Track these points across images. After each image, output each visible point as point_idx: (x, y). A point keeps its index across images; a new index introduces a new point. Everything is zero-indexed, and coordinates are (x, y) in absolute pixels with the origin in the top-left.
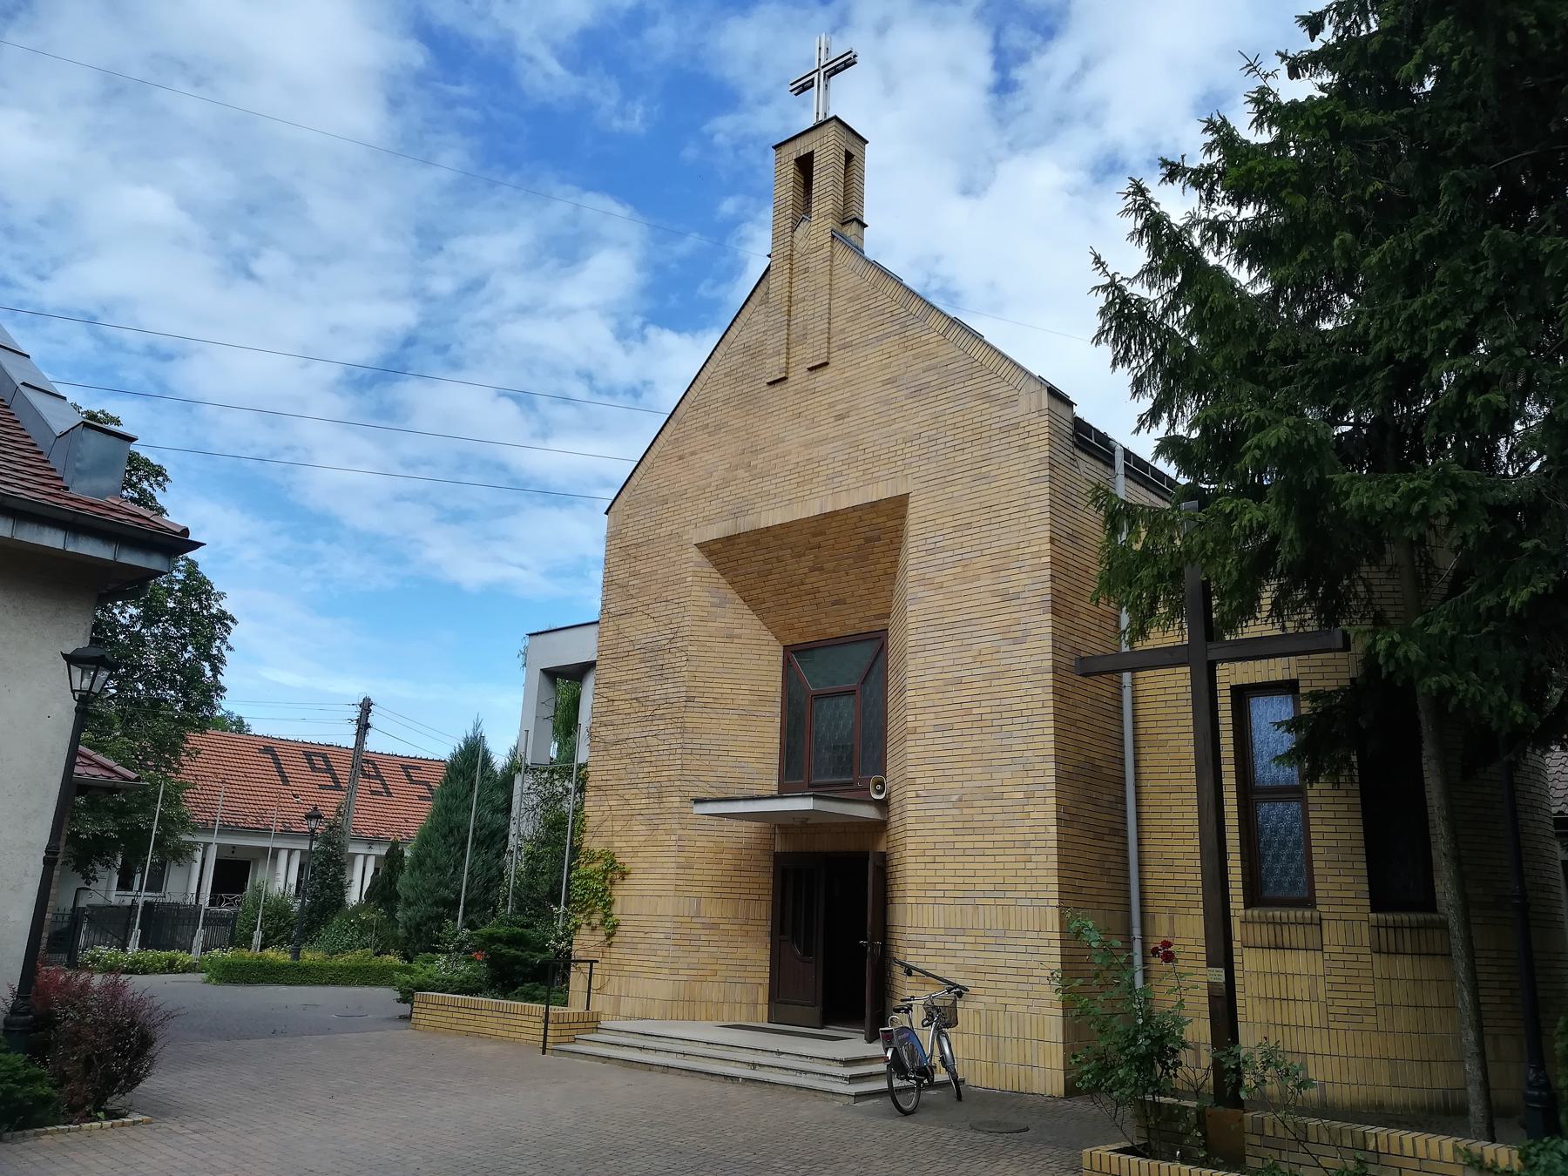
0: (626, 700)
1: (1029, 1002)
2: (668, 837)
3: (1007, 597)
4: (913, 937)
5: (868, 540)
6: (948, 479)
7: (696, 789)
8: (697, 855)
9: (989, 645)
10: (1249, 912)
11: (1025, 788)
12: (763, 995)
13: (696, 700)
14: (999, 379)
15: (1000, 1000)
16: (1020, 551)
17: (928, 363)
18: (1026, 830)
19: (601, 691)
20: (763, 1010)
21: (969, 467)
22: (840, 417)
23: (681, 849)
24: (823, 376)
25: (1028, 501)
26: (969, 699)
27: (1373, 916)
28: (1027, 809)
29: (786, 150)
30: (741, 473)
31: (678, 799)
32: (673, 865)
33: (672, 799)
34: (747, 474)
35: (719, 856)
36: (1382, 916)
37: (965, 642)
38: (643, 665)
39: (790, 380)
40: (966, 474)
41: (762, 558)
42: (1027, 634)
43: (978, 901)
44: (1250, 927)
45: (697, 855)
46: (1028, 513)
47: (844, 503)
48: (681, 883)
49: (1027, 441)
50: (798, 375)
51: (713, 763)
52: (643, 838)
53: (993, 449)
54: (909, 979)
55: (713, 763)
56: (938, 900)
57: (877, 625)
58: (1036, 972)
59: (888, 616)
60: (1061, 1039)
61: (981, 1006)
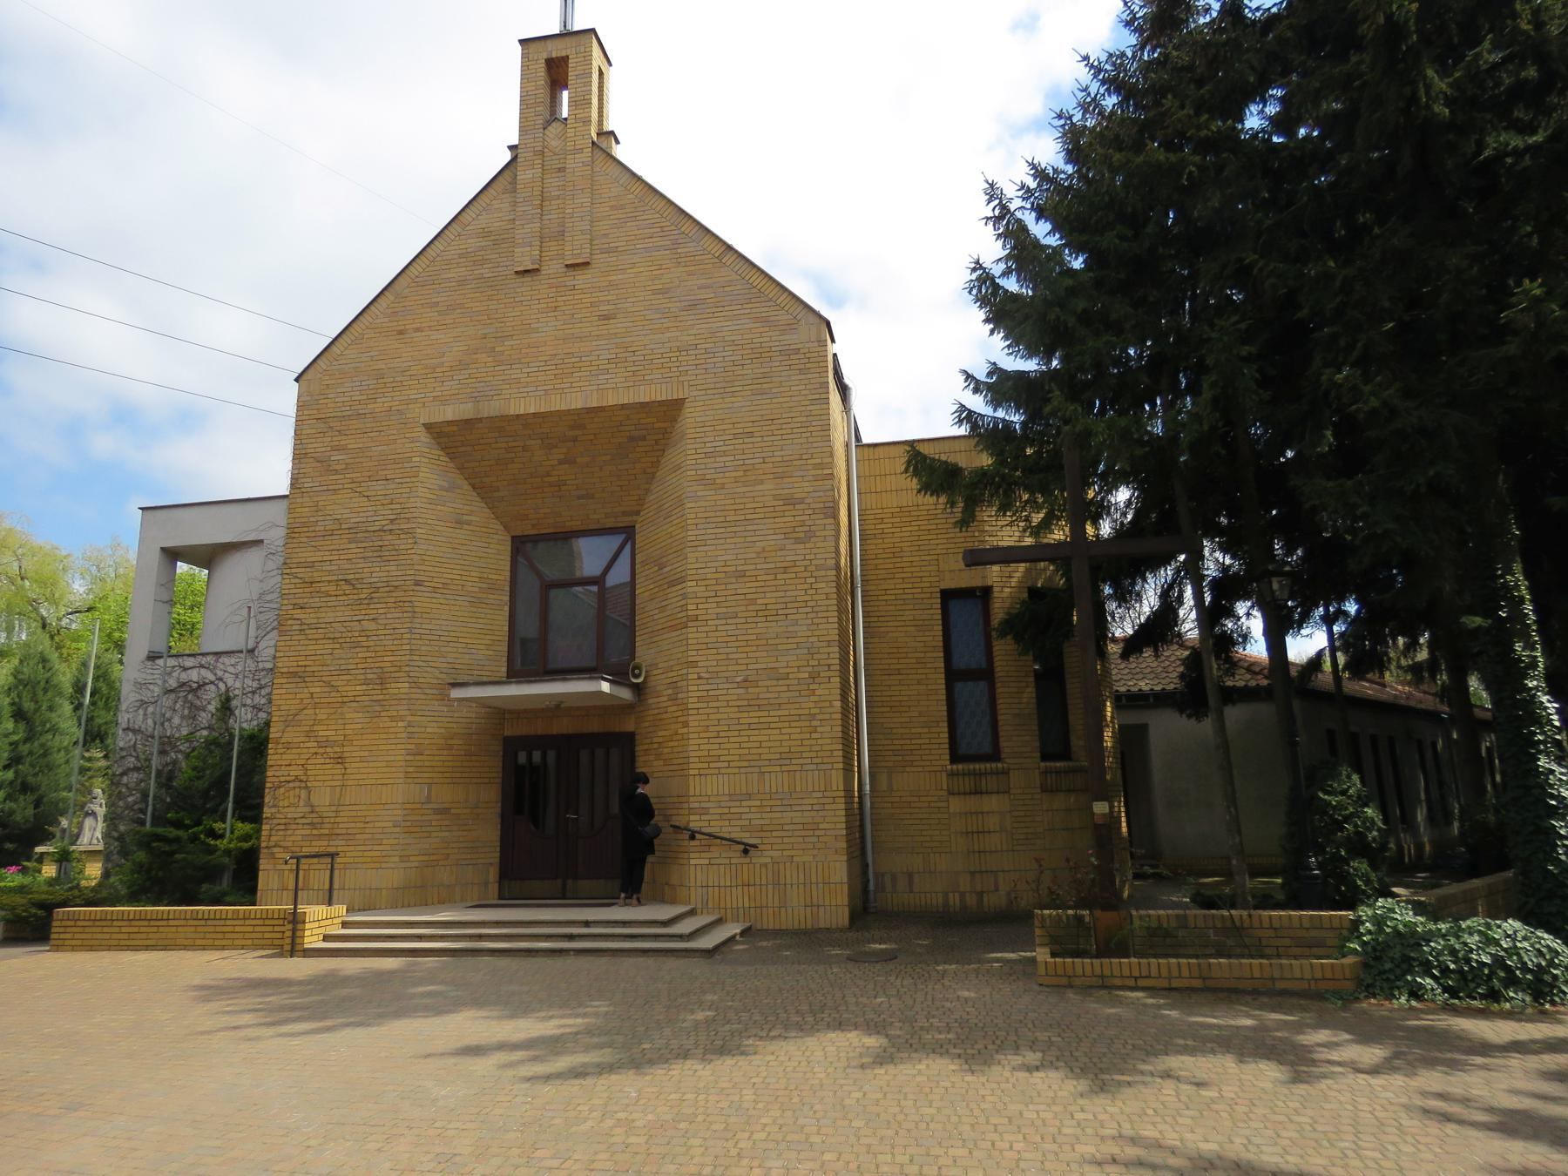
0: (329, 581)
1: (815, 852)
2: (394, 724)
3: (791, 502)
4: (697, 805)
5: (632, 439)
6: (727, 390)
7: (425, 675)
8: (427, 742)
9: (773, 543)
10: (955, 767)
11: (810, 669)
12: (493, 874)
13: (426, 584)
14: (778, 308)
15: (785, 853)
16: (803, 462)
17: (704, 281)
18: (812, 705)
19: (293, 571)
20: (494, 888)
21: (750, 382)
22: (606, 317)
23: (411, 736)
24: (582, 279)
25: (810, 418)
26: (754, 590)
27: (1043, 764)
28: (812, 687)
29: (533, 47)
30: (483, 357)
31: (407, 685)
32: (403, 752)
33: (399, 685)
34: (490, 359)
35: (450, 742)
36: (1048, 764)
37: (749, 539)
38: (353, 545)
39: (543, 272)
40: (746, 388)
41: (504, 445)
42: (810, 535)
43: (763, 769)
44: (955, 778)
45: (427, 742)
46: (810, 429)
47: (611, 400)
48: (411, 769)
49: (808, 366)
50: (553, 268)
51: (443, 649)
52: (360, 726)
53: (773, 369)
54: (693, 843)
55: (443, 649)
56: (723, 771)
57: (624, 521)
58: (821, 826)
59: (638, 513)
60: (845, 880)
61: (768, 860)
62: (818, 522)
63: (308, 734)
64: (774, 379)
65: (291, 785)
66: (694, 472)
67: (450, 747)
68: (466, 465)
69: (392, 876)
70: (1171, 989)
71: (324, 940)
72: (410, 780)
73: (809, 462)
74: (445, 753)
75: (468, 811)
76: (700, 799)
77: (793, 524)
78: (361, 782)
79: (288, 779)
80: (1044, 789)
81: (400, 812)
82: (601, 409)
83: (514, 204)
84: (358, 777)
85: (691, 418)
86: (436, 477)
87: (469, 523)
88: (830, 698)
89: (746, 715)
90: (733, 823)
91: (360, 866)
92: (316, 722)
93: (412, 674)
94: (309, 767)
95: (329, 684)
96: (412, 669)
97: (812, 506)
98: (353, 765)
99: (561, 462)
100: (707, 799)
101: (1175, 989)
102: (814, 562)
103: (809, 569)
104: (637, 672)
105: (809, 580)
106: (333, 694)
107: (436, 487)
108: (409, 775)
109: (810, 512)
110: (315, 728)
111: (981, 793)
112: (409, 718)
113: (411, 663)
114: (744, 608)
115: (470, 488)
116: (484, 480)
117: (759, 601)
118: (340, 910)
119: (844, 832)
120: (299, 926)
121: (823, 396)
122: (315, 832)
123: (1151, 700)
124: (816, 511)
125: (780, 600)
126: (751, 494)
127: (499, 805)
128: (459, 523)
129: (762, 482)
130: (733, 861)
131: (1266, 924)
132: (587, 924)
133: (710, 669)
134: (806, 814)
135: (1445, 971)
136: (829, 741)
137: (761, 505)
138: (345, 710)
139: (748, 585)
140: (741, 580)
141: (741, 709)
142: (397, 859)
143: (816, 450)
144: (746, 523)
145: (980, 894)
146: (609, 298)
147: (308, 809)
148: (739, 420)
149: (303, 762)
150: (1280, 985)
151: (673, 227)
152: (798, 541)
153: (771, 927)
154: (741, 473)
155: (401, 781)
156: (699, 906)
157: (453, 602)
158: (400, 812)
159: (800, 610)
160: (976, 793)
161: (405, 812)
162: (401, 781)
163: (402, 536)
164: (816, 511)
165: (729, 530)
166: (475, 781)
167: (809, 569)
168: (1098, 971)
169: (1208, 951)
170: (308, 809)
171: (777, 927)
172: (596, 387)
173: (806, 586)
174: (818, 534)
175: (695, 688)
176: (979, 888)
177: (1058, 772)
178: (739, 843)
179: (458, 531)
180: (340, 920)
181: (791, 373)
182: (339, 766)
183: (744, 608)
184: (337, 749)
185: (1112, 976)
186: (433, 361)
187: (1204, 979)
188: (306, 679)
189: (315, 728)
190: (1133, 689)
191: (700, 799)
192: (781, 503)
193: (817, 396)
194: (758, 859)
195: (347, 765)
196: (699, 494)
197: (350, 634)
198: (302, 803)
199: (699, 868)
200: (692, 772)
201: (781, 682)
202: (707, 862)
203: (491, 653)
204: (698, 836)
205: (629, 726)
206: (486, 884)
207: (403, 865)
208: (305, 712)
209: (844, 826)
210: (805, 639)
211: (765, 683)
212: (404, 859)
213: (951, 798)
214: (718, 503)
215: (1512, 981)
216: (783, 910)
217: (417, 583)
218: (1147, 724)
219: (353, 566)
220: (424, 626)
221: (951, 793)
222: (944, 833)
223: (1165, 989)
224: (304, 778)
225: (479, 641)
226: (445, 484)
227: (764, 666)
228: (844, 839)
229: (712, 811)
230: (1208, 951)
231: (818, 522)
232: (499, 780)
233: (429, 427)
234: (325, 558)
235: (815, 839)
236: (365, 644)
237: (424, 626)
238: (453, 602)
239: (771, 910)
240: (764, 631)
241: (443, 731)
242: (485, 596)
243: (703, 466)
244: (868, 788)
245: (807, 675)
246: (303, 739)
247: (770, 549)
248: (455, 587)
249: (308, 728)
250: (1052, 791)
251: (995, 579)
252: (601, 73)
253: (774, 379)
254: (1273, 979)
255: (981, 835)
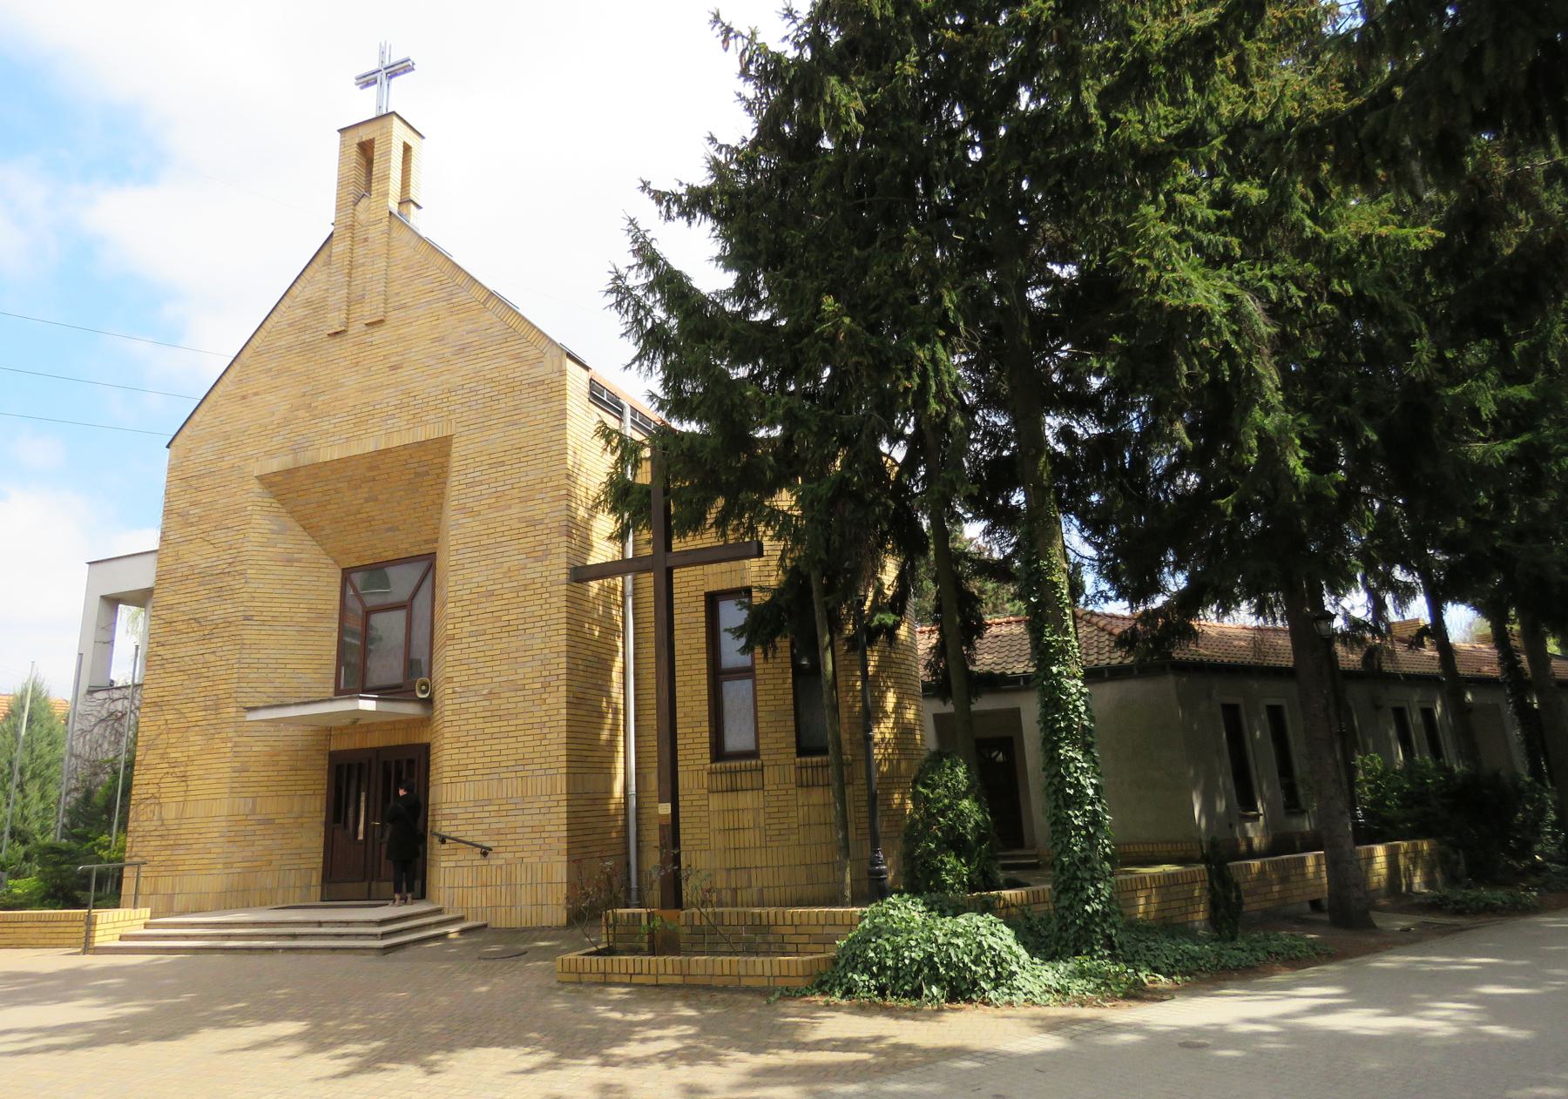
0: (183, 621)
1: (541, 853)
2: (223, 745)
3: (532, 523)
4: (447, 811)
5: (417, 474)
6: (486, 424)
7: (251, 699)
8: (253, 759)
9: (516, 563)
10: (714, 765)
11: (542, 679)
12: (316, 878)
13: (255, 618)
14: (528, 344)
15: (517, 855)
16: (544, 485)
17: (471, 326)
18: (543, 714)
19: (159, 613)
20: (316, 891)
21: (503, 415)
22: (394, 368)
23: (236, 754)
24: (378, 335)
25: (550, 444)
26: (499, 608)
27: (798, 760)
28: (544, 696)
29: (349, 134)
30: (301, 413)
31: (235, 710)
32: (229, 770)
33: (229, 710)
34: (307, 414)
35: (276, 758)
36: (803, 759)
37: (497, 561)
38: (201, 588)
39: (349, 333)
40: (500, 421)
41: (320, 489)
42: (547, 553)
43: (502, 776)
44: (714, 776)
45: (253, 759)
46: (550, 454)
47: (396, 441)
48: (236, 785)
49: (550, 395)
50: (357, 328)
51: (270, 675)
52: (198, 748)
53: (523, 401)
54: (445, 847)
55: (270, 675)
56: (469, 778)
57: (426, 549)
58: (547, 828)
59: (436, 541)
60: (565, 880)
61: (503, 862)
62: (553, 540)
63: (163, 756)
64: (523, 410)
65: (148, 802)
66: (456, 502)
67: (276, 764)
68: (295, 509)
69: (213, 882)
70: (657, 986)
71: (120, 939)
72: (235, 795)
73: (549, 484)
74: (271, 768)
75: (292, 820)
76: (451, 805)
77: (533, 544)
78: (198, 798)
79: (146, 796)
80: (800, 785)
81: (224, 824)
82: (388, 451)
83: (329, 275)
84: (197, 793)
85: (457, 452)
86: (267, 522)
87: (299, 561)
88: (558, 706)
89: (489, 725)
90: (476, 827)
91: (194, 872)
92: (169, 745)
93: (239, 700)
94: (162, 785)
95: (179, 712)
96: (239, 695)
97: (550, 526)
98: (193, 783)
99: (367, 500)
100: (455, 805)
101: (662, 985)
102: (549, 579)
103: (545, 585)
104: (424, 688)
105: (544, 596)
106: (182, 720)
107: (267, 531)
108: (235, 790)
109: (548, 531)
110: (168, 750)
111: (737, 791)
112: (238, 739)
113: (239, 690)
114: (491, 625)
115: (301, 529)
116: (311, 521)
117: (503, 618)
118: (145, 913)
119: (565, 834)
120: (92, 928)
121: (562, 422)
122: (164, 843)
123: (1022, 683)
124: (553, 530)
125: (520, 616)
126: (500, 519)
127: (324, 814)
128: (290, 561)
129: (510, 507)
130: (475, 863)
131: (813, 921)
132: (320, 924)
133: (463, 684)
134: (535, 817)
135: (883, 968)
136: (556, 747)
137: (508, 528)
138: (189, 734)
139: (496, 603)
140: (489, 599)
141: (486, 720)
142: (220, 866)
143: (554, 474)
144: (497, 545)
145: (735, 890)
146: (398, 350)
147: (159, 823)
148: (495, 451)
149: (157, 781)
150: (745, 982)
151: (449, 280)
152: (537, 560)
153: (503, 926)
154: (493, 500)
155: (226, 796)
156: (447, 906)
157: (281, 633)
158: (224, 824)
159: (537, 624)
160: (732, 791)
161: (230, 824)
162: (226, 796)
163: (237, 577)
164: (553, 530)
165: (482, 553)
166: (298, 793)
167: (545, 585)
168: (602, 969)
169: (739, 948)
170: (159, 823)
171: (508, 926)
172: (384, 432)
173: (542, 601)
174: (553, 551)
175: (450, 702)
176: (733, 886)
177: (815, 767)
178: (477, 846)
179: (288, 568)
180: (143, 922)
181: (536, 403)
182: (183, 784)
183: (491, 625)
184: (182, 769)
185: (613, 973)
186: (264, 420)
187: (684, 976)
188: (164, 708)
189: (168, 750)
190: (1009, 672)
191: (451, 805)
192: (524, 524)
193: (557, 423)
194: (496, 860)
195: (189, 783)
196: (460, 522)
197: (195, 666)
198: (155, 818)
199: (447, 870)
200: (445, 781)
201: (519, 693)
202: (453, 864)
203: (319, 676)
204: (447, 841)
205: (425, 740)
206: (309, 887)
207: (227, 871)
208: (162, 737)
209: (565, 828)
210: (539, 652)
211: (507, 695)
212: (227, 865)
213: (711, 796)
214: (475, 529)
215: (936, 979)
216: (513, 909)
217: (247, 618)
218: (1019, 708)
219: (201, 606)
220: (252, 656)
221: (710, 791)
222: (704, 830)
223: (653, 986)
224: (158, 795)
225: (307, 666)
226: (275, 528)
227: (505, 678)
228: (565, 840)
229: (459, 816)
230: (739, 948)
231: (553, 540)
232: (324, 792)
233: (260, 478)
234: (181, 601)
235: (541, 841)
236: (205, 675)
237: (252, 656)
238: (281, 633)
239: (503, 909)
240: (506, 645)
241: (268, 749)
242: (313, 624)
243: (464, 496)
244: (633, 789)
245: (539, 685)
246: (158, 761)
247: (515, 568)
248: (284, 619)
249: (161, 751)
250: (808, 786)
251: (753, 579)
252: (407, 149)
253: (523, 410)
254: (739, 976)
255: (736, 832)
